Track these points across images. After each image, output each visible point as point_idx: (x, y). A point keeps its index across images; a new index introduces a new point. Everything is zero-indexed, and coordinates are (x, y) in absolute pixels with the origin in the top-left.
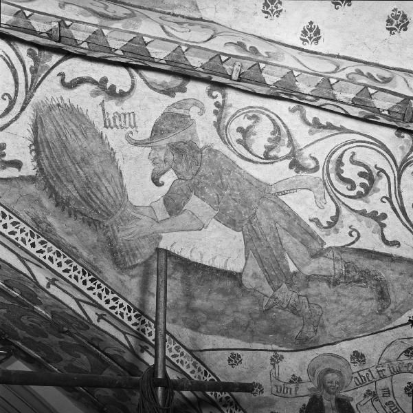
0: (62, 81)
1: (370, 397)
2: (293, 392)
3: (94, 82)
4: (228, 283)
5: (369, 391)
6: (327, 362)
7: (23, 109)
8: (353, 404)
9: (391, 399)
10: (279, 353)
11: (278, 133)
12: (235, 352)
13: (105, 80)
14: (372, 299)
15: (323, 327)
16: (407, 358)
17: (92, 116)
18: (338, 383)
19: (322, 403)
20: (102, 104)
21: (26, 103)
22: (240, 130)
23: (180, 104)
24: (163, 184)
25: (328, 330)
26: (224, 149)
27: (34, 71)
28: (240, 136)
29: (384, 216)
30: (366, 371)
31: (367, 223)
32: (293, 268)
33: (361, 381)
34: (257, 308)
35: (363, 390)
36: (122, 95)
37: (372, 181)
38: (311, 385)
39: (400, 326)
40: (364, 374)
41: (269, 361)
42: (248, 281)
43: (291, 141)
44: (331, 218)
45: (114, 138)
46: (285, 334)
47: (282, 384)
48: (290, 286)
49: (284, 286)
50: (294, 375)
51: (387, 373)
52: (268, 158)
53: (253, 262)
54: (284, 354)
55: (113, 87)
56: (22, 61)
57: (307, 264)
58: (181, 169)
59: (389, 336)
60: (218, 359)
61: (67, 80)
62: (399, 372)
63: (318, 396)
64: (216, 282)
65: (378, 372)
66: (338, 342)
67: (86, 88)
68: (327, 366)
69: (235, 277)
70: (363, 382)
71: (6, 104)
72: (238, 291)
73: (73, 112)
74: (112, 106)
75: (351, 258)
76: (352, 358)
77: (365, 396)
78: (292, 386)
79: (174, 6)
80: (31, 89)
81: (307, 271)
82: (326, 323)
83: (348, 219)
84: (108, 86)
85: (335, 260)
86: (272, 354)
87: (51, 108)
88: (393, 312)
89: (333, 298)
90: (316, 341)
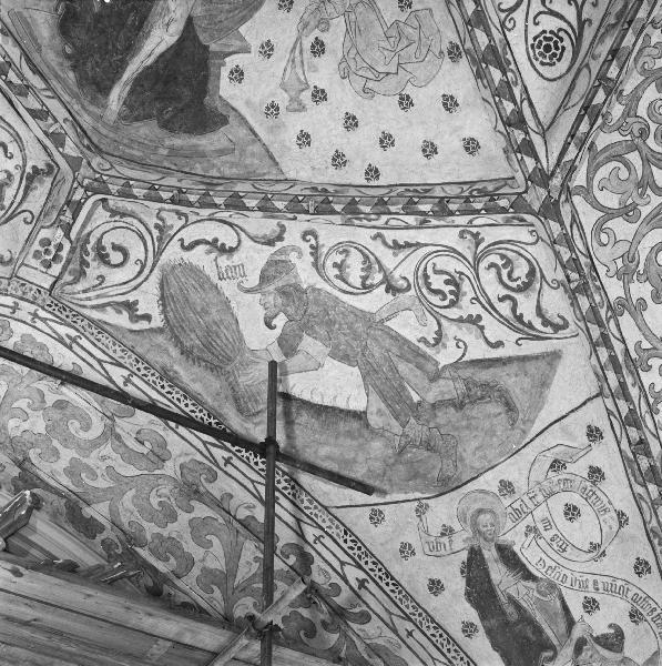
0: (182, 245)
2: (448, 548)
3: (207, 243)
4: (355, 425)
5: (528, 527)
7: (151, 271)
8: (516, 549)
11: (369, 262)
12: (375, 507)
13: (216, 240)
14: (500, 414)
15: (462, 460)
17: (208, 271)
18: (492, 525)
20: (216, 260)
21: (154, 265)
22: (335, 265)
23: (282, 251)
24: (275, 327)
25: (467, 461)
26: (321, 284)
27: (160, 239)
28: (336, 272)
29: (479, 317)
30: (519, 502)
31: (468, 329)
32: (416, 398)
34: (390, 451)
35: (522, 527)
36: (232, 250)
37: (457, 286)
39: (537, 436)
40: (516, 506)
42: (374, 420)
43: (381, 268)
44: (436, 333)
45: (227, 288)
46: (424, 477)
47: (433, 539)
48: (417, 418)
49: (412, 420)
50: (444, 525)
51: (540, 498)
52: (367, 288)
53: (374, 397)
55: (223, 244)
56: (150, 233)
57: (429, 390)
58: (291, 310)
59: (529, 453)
60: (358, 517)
61: (186, 244)
62: (552, 494)
64: (342, 424)
67: (201, 248)
69: (359, 416)
70: (518, 514)
71: (138, 268)
72: (366, 433)
73: (193, 270)
74: (224, 261)
75: (467, 373)
76: (500, 491)
78: (445, 540)
79: (265, 174)
80: (158, 254)
81: (431, 397)
82: (464, 455)
83: (451, 330)
84: (219, 243)
85: (454, 379)
86: (416, 503)
87: (174, 268)
88: (524, 423)
89: (464, 423)
90: (458, 479)
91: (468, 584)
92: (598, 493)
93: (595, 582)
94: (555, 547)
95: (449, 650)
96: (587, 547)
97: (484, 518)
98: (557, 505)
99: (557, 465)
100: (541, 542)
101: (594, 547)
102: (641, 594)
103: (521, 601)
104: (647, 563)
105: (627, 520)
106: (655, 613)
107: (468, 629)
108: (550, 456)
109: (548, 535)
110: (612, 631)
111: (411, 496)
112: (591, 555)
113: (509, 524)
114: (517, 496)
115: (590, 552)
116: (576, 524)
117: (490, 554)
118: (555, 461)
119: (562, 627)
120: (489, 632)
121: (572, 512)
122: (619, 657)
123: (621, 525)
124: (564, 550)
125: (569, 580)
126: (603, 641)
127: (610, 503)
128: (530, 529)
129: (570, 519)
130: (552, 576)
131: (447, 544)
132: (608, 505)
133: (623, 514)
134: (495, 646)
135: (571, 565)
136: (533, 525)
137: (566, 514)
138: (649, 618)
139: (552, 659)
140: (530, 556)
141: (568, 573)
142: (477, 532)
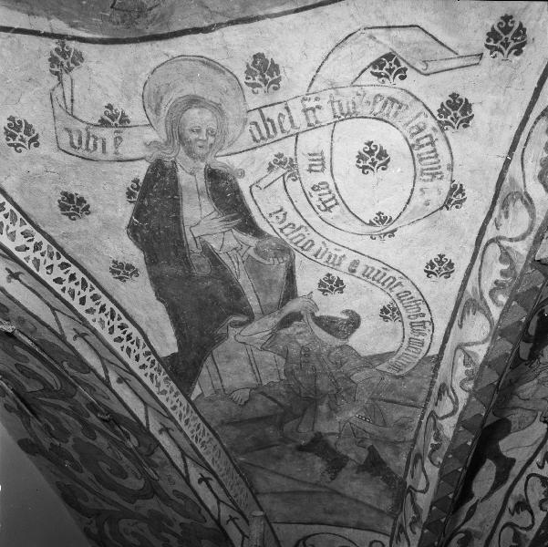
1: (282, 171)
6: (190, 78)
8: (244, 185)
9: (326, 177)
10: (73, 45)
16: (375, 80)
18: (211, 133)
19: (175, 180)
30: (279, 109)
33: (264, 131)
35: (268, 154)
38: (151, 135)
40: (272, 113)
41: (45, 65)
47: (82, 127)
50: (110, 107)
51: (325, 115)
54: (85, 48)
62: (350, 115)
63: (168, 164)
65: (305, 111)
66: (219, 26)
68: (191, 89)
76: (249, 72)
77: (271, 168)
78: (107, 134)
91: (137, 214)
92: (441, 147)
93: (356, 263)
94: (315, 200)
95: (83, 301)
96: (369, 215)
97: (195, 117)
98: (354, 137)
99: (388, 66)
100: (294, 187)
101: (382, 219)
102: (415, 293)
103: (223, 257)
104: (451, 265)
105: (461, 202)
106: (420, 319)
107: (122, 270)
108: (384, 43)
109: (310, 180)
110: (345, 317)
111: (42, 24)
112: (372, 229)
113: (245, 140)
114: (280, 96)
115: (371, 224)
116: (371, 177)
117: (190, 178)
118: (389, 56)
119: (275, 298)
120: (156, 281)
121: (374, 158)
122: (339, 342)
123: (447, 204)
124: (328, 209)
125: (315, 248)
126: (328, 324)
127: (451, 168)
128: (280, 161)
129: (364, 168)
130: (289, 237)
131: (110, 144)
132: (444, 169)
133: (461, 191)
134: (161, 295)
135: (328, 232)
136: (289, 154)
137: (360, 157)
138: (407, 321)
139: (242, 324)
140: (265, 204)
141: (318, 240)
142: (177, 135)
